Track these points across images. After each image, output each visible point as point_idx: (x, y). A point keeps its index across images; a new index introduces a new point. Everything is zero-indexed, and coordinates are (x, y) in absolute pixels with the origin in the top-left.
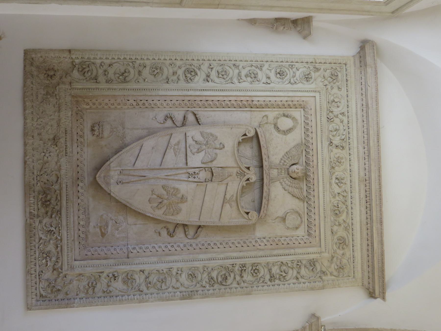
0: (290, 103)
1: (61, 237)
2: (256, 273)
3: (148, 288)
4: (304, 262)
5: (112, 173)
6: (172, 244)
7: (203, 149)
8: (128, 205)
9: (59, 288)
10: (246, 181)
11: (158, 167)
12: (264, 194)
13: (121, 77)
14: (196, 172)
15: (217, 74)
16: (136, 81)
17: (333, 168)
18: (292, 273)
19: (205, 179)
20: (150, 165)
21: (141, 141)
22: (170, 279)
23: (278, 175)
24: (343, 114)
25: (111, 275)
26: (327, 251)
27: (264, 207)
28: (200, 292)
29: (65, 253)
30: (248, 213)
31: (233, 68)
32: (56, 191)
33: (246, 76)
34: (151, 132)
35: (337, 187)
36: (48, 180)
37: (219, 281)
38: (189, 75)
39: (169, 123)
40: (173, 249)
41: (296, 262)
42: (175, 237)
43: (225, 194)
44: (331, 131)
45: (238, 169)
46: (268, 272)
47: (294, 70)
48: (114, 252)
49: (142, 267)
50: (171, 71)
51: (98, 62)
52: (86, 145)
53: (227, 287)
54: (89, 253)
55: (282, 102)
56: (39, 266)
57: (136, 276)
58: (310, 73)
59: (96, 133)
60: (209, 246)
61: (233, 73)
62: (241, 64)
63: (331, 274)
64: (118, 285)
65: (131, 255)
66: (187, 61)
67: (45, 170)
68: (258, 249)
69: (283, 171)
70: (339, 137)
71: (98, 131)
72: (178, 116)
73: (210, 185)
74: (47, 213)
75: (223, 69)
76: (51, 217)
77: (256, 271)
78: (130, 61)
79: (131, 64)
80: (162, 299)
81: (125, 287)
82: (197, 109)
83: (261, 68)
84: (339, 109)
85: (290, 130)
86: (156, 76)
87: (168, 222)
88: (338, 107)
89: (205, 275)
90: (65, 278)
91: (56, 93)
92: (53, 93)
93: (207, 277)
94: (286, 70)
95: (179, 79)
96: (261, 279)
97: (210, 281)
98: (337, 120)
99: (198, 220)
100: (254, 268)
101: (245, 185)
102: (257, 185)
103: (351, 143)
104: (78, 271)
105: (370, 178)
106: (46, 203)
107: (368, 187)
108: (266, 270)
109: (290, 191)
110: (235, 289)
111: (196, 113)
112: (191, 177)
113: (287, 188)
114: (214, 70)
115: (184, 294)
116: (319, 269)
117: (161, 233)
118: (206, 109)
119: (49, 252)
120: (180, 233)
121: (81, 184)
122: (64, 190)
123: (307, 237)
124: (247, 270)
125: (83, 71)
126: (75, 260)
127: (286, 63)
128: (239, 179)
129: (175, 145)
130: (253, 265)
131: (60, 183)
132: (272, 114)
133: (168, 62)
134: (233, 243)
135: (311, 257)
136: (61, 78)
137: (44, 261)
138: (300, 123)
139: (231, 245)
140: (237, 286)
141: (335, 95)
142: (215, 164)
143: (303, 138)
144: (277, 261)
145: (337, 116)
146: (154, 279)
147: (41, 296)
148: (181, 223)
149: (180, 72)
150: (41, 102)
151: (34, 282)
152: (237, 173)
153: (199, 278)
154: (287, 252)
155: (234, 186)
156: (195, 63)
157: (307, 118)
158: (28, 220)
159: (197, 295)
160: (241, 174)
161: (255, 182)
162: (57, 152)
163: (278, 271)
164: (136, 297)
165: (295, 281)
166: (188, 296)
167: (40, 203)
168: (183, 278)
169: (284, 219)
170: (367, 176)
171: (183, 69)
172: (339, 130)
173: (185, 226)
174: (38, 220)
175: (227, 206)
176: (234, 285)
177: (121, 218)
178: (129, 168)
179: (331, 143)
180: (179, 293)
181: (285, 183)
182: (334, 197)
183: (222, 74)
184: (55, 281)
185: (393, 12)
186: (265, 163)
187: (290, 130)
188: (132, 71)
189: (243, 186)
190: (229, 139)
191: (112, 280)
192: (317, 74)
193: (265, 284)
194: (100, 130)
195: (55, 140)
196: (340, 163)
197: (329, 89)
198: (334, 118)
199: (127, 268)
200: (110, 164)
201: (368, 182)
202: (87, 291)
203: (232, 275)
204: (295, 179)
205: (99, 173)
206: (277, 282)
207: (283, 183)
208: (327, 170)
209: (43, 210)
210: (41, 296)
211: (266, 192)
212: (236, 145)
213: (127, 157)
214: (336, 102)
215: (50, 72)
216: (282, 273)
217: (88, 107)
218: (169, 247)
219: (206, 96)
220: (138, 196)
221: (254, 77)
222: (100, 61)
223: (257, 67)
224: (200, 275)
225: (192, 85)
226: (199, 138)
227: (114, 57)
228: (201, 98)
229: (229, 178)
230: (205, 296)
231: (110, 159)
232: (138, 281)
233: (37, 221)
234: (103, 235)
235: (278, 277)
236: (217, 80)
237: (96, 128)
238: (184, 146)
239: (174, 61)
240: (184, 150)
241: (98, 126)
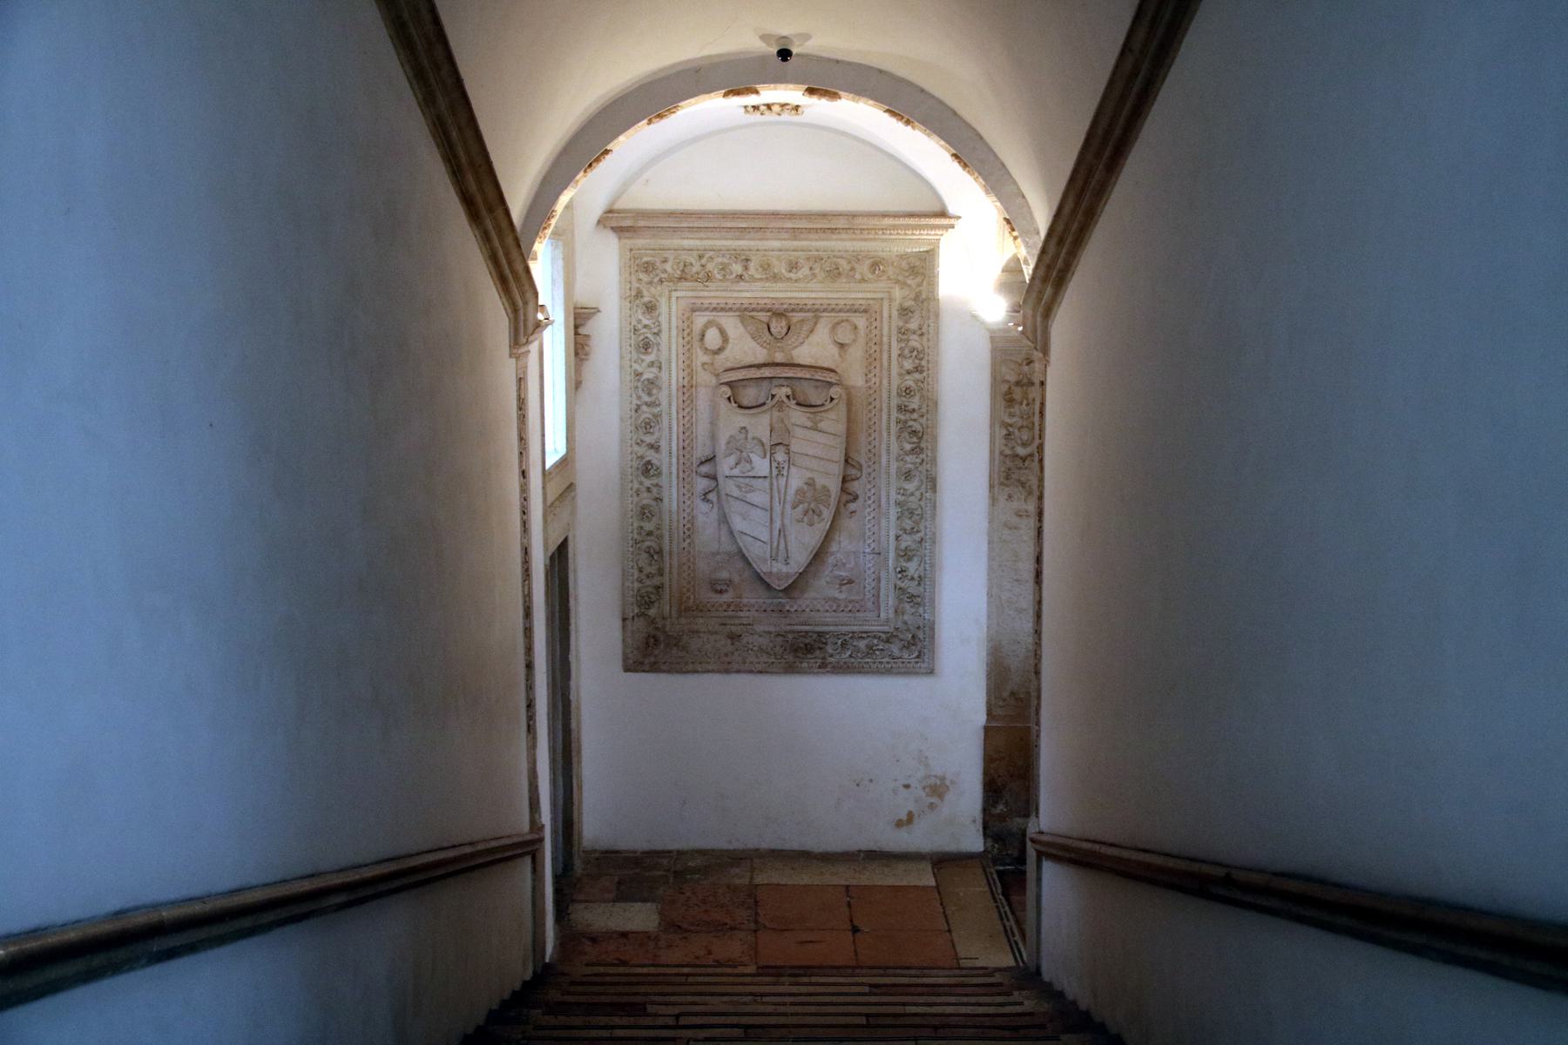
5: (775, 570)
18: (915, 342)
24: (701, 257)
33: (650, 394)
34: (724, 519)
39: (712, 496)
49: (892, 539)
50: (646, 495)
51: (636, 585)
57: (903, 545)
61: (646, 412)
62: (636, 402)
64: (912, 567)
72: (702, 484)
73: (793, 448)
75: (644, 425)
80: (934, 516)
83: (638, 374)
85: (722, 332)
89: (908, 458)
98: (710, 267)
104: (891, 615)
106: (809, 649)
120: (855, 487)
125: (650, 604)
130: (899, 395)
133: (636, 499)
135: (895, 313)
146: (908, 524)
149: (648, 483)
154: (886, 347)
156: (635, 464)
166: (932, 483)
168: (911, 487)
173: (844, 480)
175: (822, 425)
176: (923, 421)
177: (831, 560)
183: (647, 426)
187: (722, 332)
188: (647, 544)
190: (733, 421)
192: (645, 293)
195: (734, 637)
199: (892, 555)
206: (924, 363)
208: (779, 285)
213: (755, 551)
220: (802, 541)
221: (651, 385)
225: (665, 470)
226: (732, 460)
230: (934, 461)
234: (850, 582)
236: (657, 435)
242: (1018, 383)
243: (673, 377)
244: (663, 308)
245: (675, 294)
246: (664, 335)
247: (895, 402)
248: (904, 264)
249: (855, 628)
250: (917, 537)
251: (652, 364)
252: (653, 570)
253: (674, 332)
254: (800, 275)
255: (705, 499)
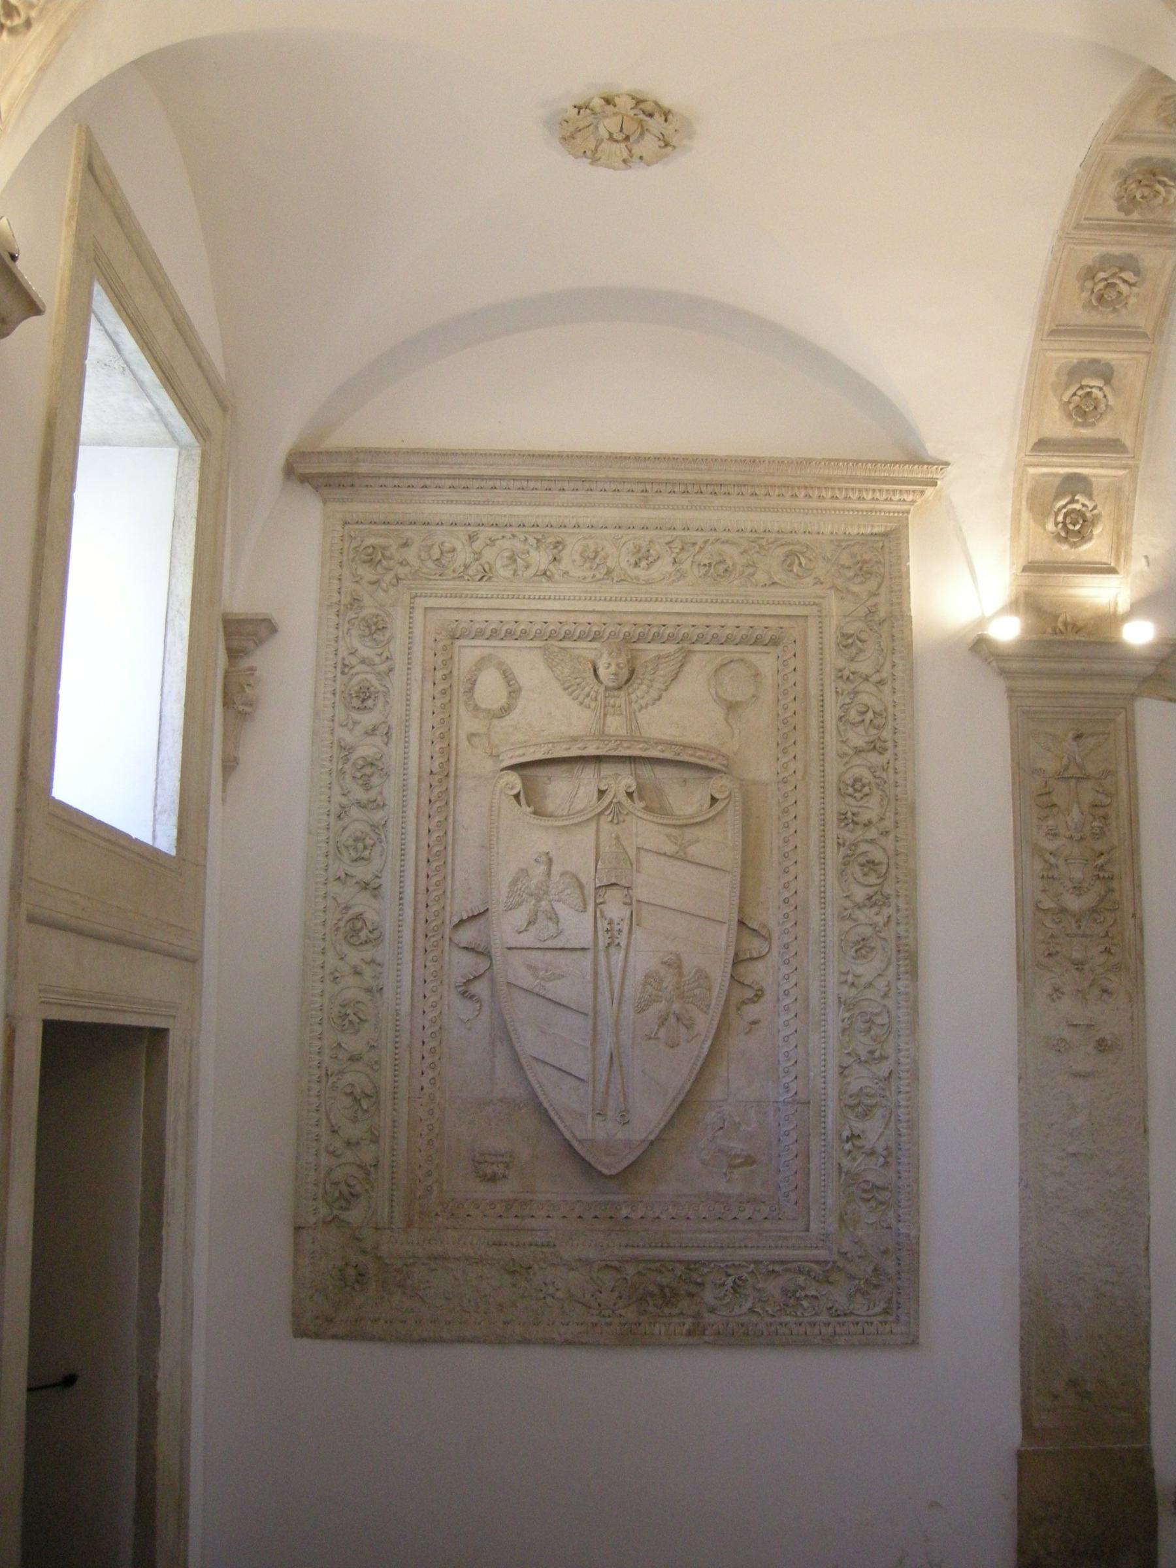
0: (439, 674)
1: (750, 1262)
2: (864, 786)
3: (883, 1058)
4: (841, 663)
6: (781, 992)
7: (548, 908)
8: (680, 1098)
9: (870, 1269)
10: (633, 801)
11: (591, 1022)
12: (668, 755)
13: (365, 1105)
14: (606, 926)
15: (359, 863)
16: (376, 1067)
17: (609, 572)
19: (625, 904)
20: (584, 1040)
21: (523, 1061)
22: (865, 1003)
23: (621, 714)
24: (472, 538)
25: (848, 1146)
26: (817, 601)
27: (700, 758)
28: (901, 930)
29: (792, 1254)
30: (714, 800)
31: (347, 820)
32: (639, 1273)
33: (367, 787)
34: (503, 1034)
35: (659, 563)
36: (612, 1291)
37: (879, 881)
38: (363, 935)
40: (794, 992)
41: (841, 684)
42: (764, 985)
43: (665, 854)
44: (515, 571)
45: (602, 818)
46: (863, 755)
47: (353, 660)
48: (794, 1136)
50: (351, 980)
51: (325, 1159)
52: (529, 1196)
53: (892, 862)
54: (793, 1196)
55: (437, 696)
56: (816, 1314)
57: (854, 1087)
58: (363, 619)
59: (500, 1169)
60: (792, 901)
62: (338, 798)
63: (875, 595)
64: (873, 1130)
65: (802, 1097)
66: (328, 938)
67: (588, 1296)
68: (803, 778)
69: (612, 701)
70: (533, 553)
71: (494, 1166)
73: (641, 893)
74: (691, 1295)
75: (349, 846)
76: (702, 1284)
77: (858, 786)
78: (324, 1082)
79: (333, 1079)
80: (914, 1026)
81: (879, 1112)
82: (448, 915)
83: (347, 750)
84: (459, 546)
85: (508, 676)
86: (363, 1017)
87: (727, 1001)
88: (454, 550)
89: (860, 915)
90: (849, 1255)
91: (399, 1263)
92: (399, 1271)
93: (866, 910)
94: (354, 681)
95: (373, 961)
96: (877, 774)
97: (875, 904)
98: (488, 555)
99: (725, 927)
100: (850, 791)
101: (642, 804)
102: (646, 772)
103: (547, 520)
104: (833, 1226)
105: (640, 482)
106: (668, 1296)
107: (663, 487)
108: (857, 761)
109: (663, 687)
110: (900, 844)
111: (456, 920)
112: (617, 941)
113: (654, 693)
114: (352, 871)
115: (902, 969)
116: (861, 625)
117: (751, 1020)
118: (448, 894)
119: (785, 1291)
120: (757, 973)
121: (625, 1212)
122: (638, 1252)
123: (781, 647)
124: (855, 810)
126: (807, 1230)
127: (338, 682)
128: (628, 818)
129: (537, 978)
130: (841, 794)
131: (620, 1261)
132: (468, 723)
134: (786, 841)
136: (364, 1252)
137: (805, 1304)
138: (491, 651)
139: (791, 847)
140: (891, 837)
141: (423, 554)
142: (587, 877)
143: (531, 644)
144: (834, 732)
145: (478, 556)
146: (862, 1045)
147: (886, 1312)
148: (729, 970)
149: (355, 956)
150: (423, 1300)
151: (852, 1329)
152: (612, 821)
153: (868, 931)
154: (814, 703)
155: (645, 832)
157: (479, 634)
158: (706, 1338)
159: (907, 937)
160: (616, 813)
161: (637, 777)
162: (544, 1266)
163: (860, 729)
164: (903, 1089)
165: (887, 689)
166: (909, 960)
167: (666, 1310)
168: (865, 970)
169: (732, 707)
170: (634, 487)
171: (345, 948)
172: (513, 552)
173: (737, 961)
174: (706, 1315)
175: (694, 851)
176: (888, 842)
178: (590, 1093)
179: (545, 573)
180: (901, 983)
181: (643, 698)
182: (683, 575)
183: (361, 849)
184: (852, 1277)
185: (224, 409)
186: (591, 751)
187: (508, 676)
188: (349, 1078)
189: (647, 809)
191: (858, 1143)
192: (367, 600)
193: (891, 765)
194: (494, 1159)
195: (517, 1270)
196: (597, 553)
197: (407, 570)
198: (482, 561)
200: (577, 1140)
201: (648, 487)
202: (883, 1203)
203: (864, 847)
204: (632, 672)
205: (599, 1168)
206: (886, 734)
207: (642, 702)
208: (617, 589)
209: (685, 1303)
210: (888, 1313)
211: (663, 751)
212: (543, 823)
213: (561, 1097)
214: (442, 553)
215: (353, 1278)
216: (867, 721)
217: (435, 1188)
218: (787, 1001)
219: (416, 893)
222: (324, 1154)
223: (346, 759)
224: (860, 929)
225: (388, 926)
226: (520, 916)
227: (313, 1122)
228: (421, 907)
229: (625, 844)
230: (912, 917)
231: (565, 1139)
232: (866, 1082)
233: (709, 1318)
234: (749, 1161)
235: (875, 731)
237: (489, 1171)
238: (539, 953)
239: (328, 971)
240: (549, 956)
241: (483, 1166)
242: (1061, 777)
243: (411, 754)
244: (399, 625)
245: (421, 603)
246: (397, 681)
247: (834, 806)
248: (845, 559)
249: (760, 1254)
250: (883, 1069)
251: (373, 732)
252: (355, 1131)
253: (417, 673)
254: (655, 572)
255: (466, 995)
